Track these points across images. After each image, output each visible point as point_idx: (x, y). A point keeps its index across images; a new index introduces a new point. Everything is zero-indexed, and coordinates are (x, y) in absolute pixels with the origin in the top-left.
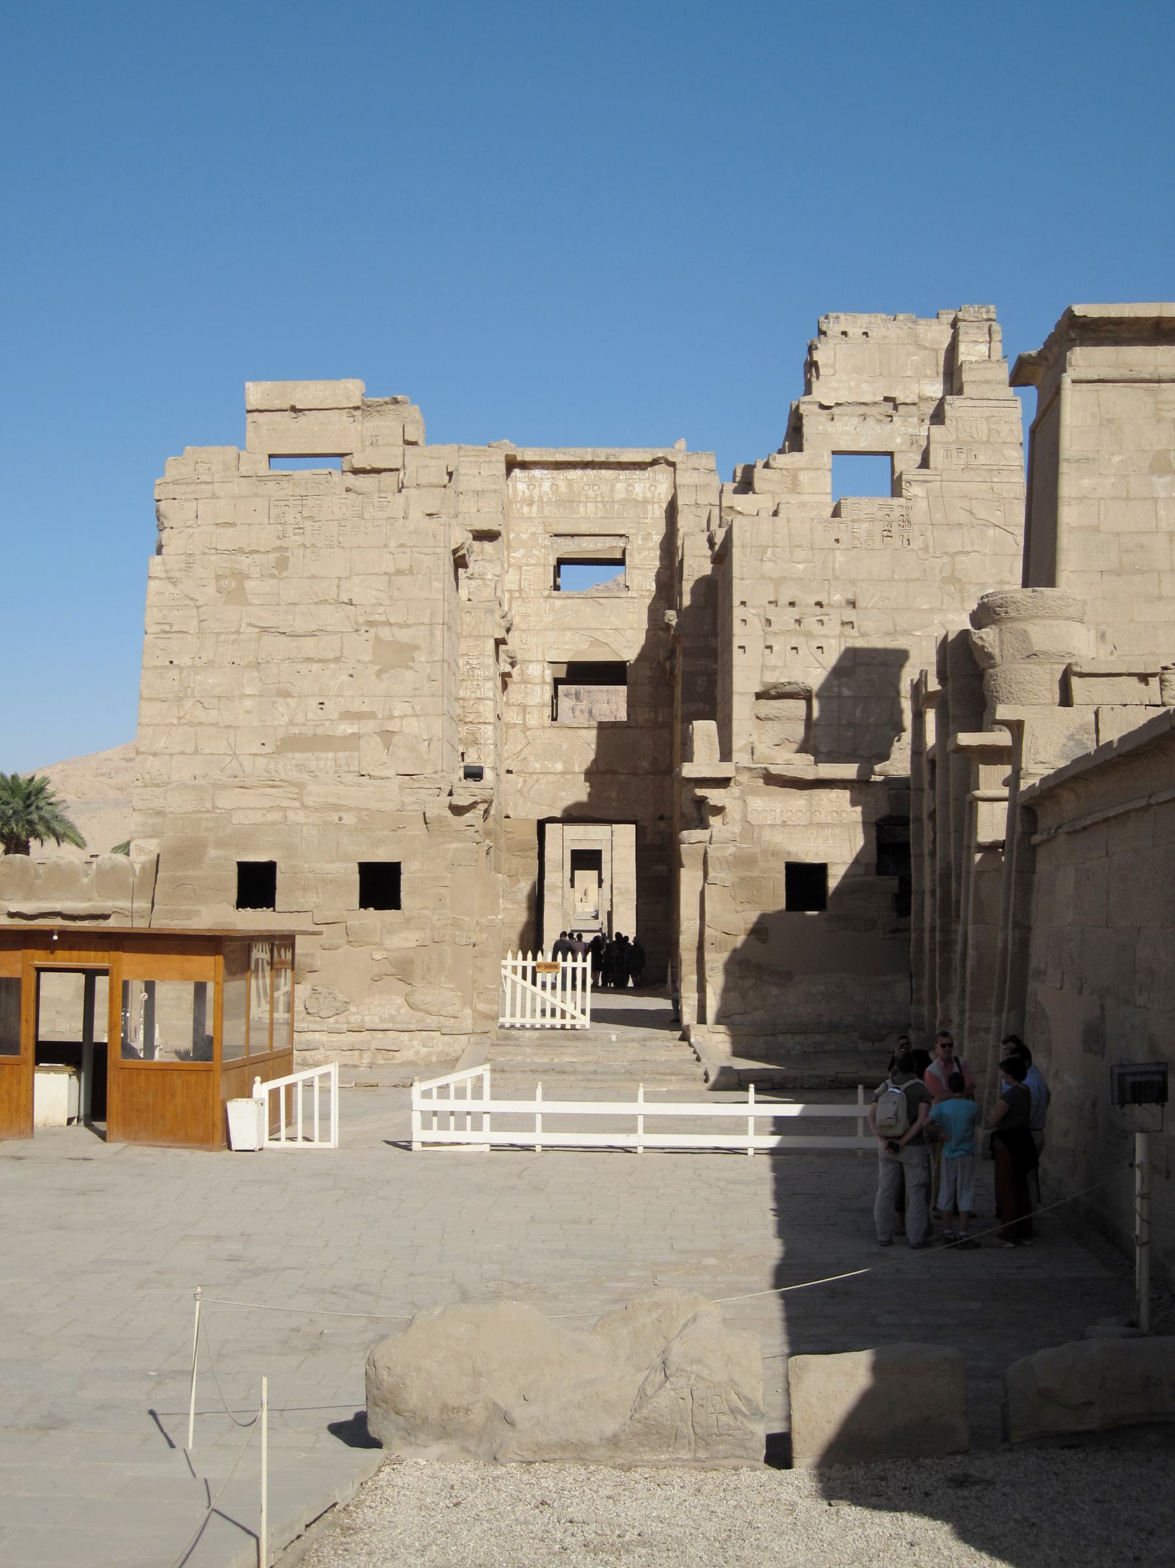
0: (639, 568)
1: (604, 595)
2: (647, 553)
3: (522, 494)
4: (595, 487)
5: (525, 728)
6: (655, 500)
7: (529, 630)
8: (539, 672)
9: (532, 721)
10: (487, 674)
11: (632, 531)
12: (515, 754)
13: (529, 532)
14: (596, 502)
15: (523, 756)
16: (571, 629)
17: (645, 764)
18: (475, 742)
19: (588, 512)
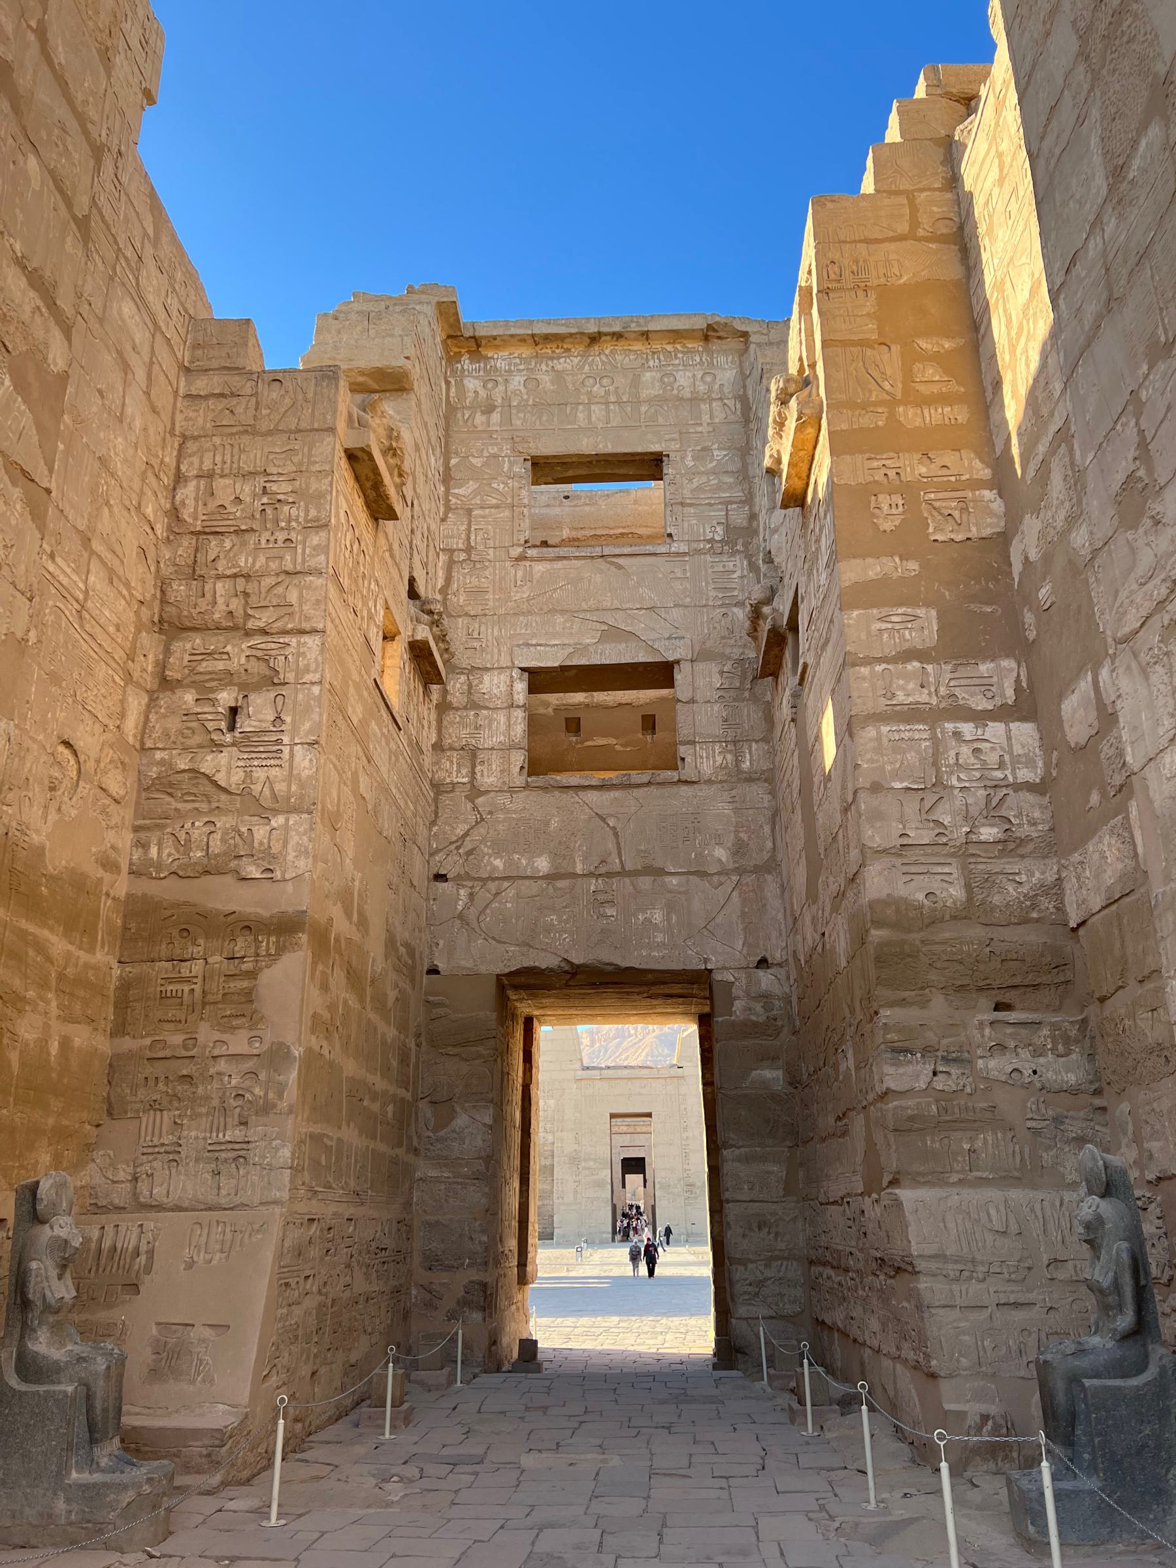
0: (691, 505)
1: (627, 550)
2: (704, 479)
3: (471, 394)
4: (605, 381)
5: (474, 792)
6: (714, 396)
8: (503, 688)
9: (488, 778)
10: (313, 513)
12: (451, 843)
13: (486, 454)
14: (607, 403)
15: (468, 845)
16: (563, 612)
17: (721, 853)
18: (272, 681)
19: (593, 419)
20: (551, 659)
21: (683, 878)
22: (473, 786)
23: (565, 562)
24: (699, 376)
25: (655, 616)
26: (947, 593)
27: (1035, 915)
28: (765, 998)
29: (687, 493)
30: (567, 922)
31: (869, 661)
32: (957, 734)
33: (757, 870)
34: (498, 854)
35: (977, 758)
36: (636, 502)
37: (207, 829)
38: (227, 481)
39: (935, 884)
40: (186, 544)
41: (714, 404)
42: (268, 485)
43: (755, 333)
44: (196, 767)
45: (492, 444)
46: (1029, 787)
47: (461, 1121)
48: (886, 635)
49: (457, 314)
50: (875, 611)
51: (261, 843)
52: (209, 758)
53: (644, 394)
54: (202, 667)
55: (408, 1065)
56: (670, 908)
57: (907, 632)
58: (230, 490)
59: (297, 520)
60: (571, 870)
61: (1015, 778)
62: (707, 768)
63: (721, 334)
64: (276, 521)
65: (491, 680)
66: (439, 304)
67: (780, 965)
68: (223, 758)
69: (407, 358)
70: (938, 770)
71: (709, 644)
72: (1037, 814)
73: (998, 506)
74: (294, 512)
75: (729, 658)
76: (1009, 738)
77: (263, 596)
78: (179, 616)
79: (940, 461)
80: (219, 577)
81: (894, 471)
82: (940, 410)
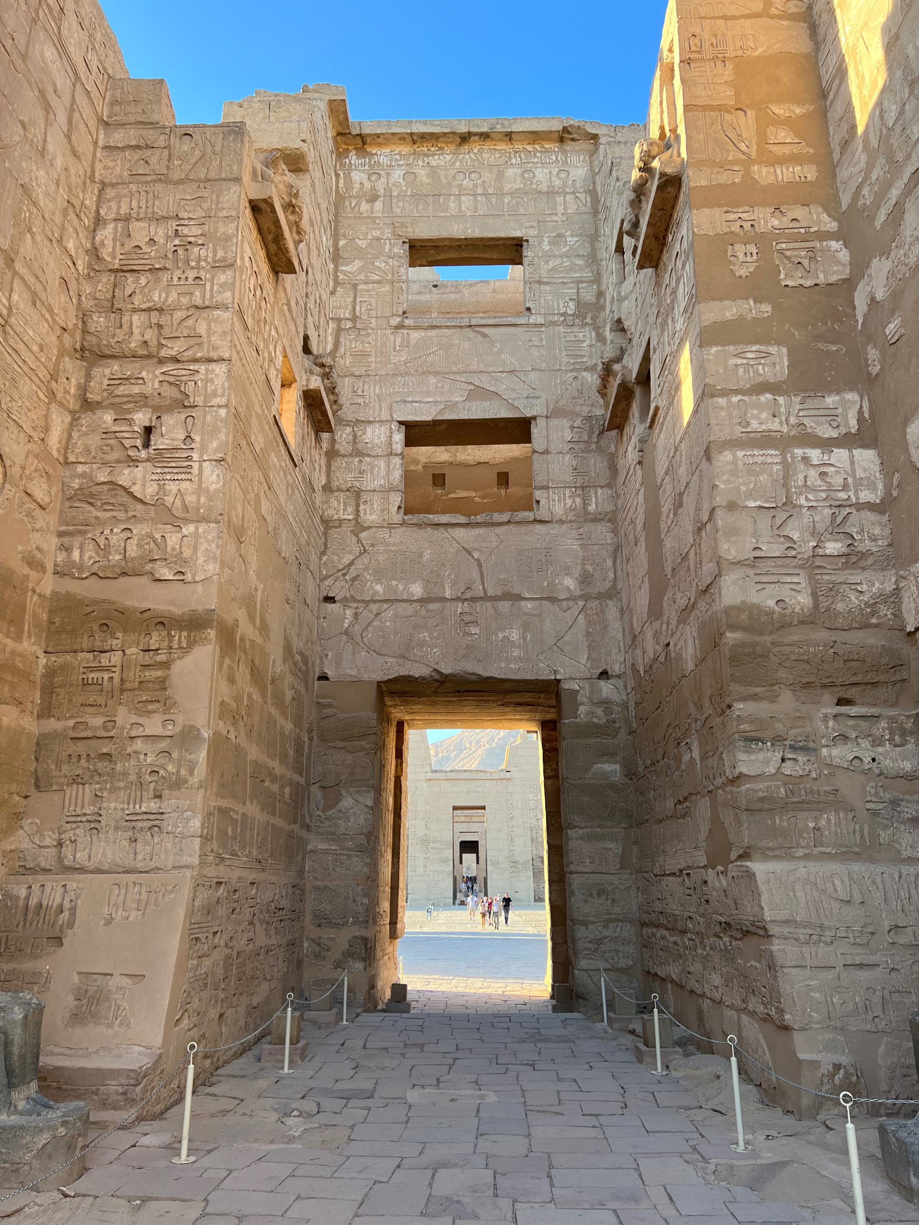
0: (547, 283)
1: (490, 322)
2: (558, 261)
3: (357, 186)
4: (473, 176)
5: (359, 527)
6: (567, 190)
7: (368, 375)
8: (383, 438)
9: (370, 516)
10: (220, 254)
11: (533, 232)
12: (339, 571)
13: (369, 237)
14: (475, 195)
15: (353, 573)
16: (435, 373)
17: (569, 582)
18: (182, 404)
19: (463, 208)
20: (425, 414)
21: (537, 602)
22: (357, 522)
23: (438, 331)
24: (555, 173)
25: (515, 378)
26: (796, 333)
27: (874, 621)
28: (606, 703)
29: (543, 273)
30: (437, 638)
31: (726, 393)
32: (805, 459)
33: (600, 596)
34: (378, 581)
35: (823, 480)
36: (494, 291)
37: (124, 535)
38: (142, 224)
39: (784, 592)
40: (105, 282)
41: (568, 197)
42: (179, 228)
43: (604, 135)
44: (114, 479)
45: (374, 229)
46: (870, 507)
47: (347, 802)
48: (741, 370)
49: (346, 112)
50: (731, 348)
51: (174, 549)
52: (126, 472)
53: (507, 187)
54: (120, 390)
55: (302, 755)
56: (525, 628)
57: (760, 367)
58: (145, 233)
59: (206, 260)
60: (441, 595)
61: (858, 498)
62: (558, 510)
63: (575, 136)
64: (187, 261)
65: (374, 432)
66: (331, 102)
67: (619, 677)
68: (139, 472)
69: (304, 141)
70: (788, 491)
71: (561, 403)
72: (877, 531)
73: (844, 255)
74: (203, 253)
75: (579, 415)
76: (852, 463)
77: (175, 327)
78: (99, 345)
79: (791, 215)
80: (135, 310)
81: (749, 223)
82: (791, 169)
